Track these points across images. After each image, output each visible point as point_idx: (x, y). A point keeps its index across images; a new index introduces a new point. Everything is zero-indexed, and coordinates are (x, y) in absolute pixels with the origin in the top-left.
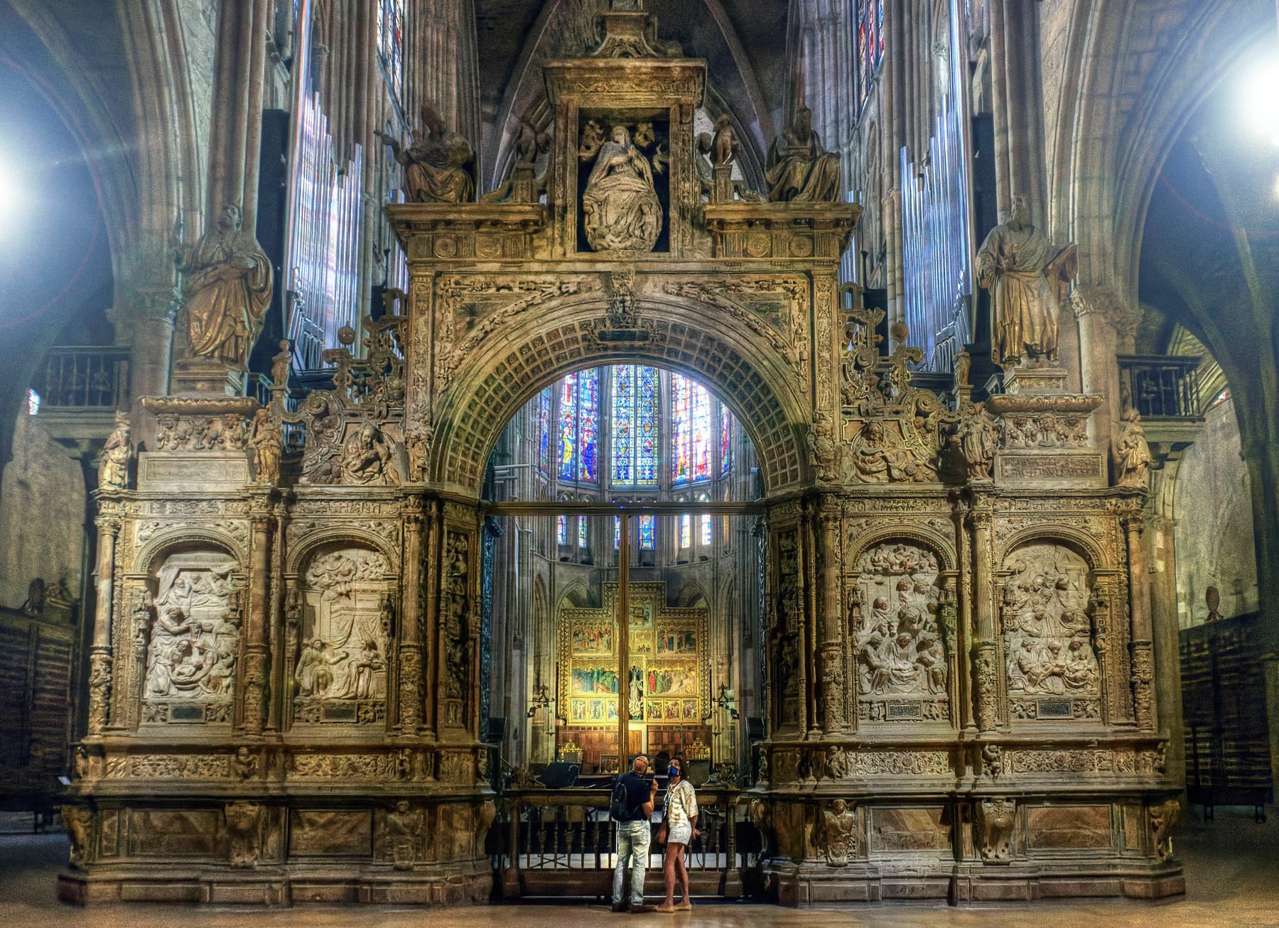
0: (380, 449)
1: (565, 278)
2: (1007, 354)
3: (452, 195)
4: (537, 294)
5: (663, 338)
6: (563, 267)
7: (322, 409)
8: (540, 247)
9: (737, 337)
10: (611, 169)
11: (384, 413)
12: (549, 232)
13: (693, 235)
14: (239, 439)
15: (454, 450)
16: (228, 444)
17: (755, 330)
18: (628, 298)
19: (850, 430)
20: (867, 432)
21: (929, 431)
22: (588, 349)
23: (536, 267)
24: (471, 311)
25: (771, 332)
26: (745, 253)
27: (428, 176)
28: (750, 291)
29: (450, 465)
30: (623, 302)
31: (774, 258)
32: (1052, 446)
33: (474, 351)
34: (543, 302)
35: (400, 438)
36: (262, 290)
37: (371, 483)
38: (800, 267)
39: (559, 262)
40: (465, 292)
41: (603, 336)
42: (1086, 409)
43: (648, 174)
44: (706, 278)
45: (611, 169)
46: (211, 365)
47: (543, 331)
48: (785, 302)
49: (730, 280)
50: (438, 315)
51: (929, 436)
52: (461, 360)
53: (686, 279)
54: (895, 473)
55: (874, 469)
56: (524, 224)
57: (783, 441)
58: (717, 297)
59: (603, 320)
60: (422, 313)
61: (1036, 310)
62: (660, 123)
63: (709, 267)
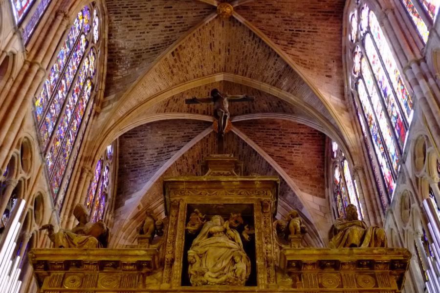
10: (210, 235)
13: (276, 276)
56: (139, 265)
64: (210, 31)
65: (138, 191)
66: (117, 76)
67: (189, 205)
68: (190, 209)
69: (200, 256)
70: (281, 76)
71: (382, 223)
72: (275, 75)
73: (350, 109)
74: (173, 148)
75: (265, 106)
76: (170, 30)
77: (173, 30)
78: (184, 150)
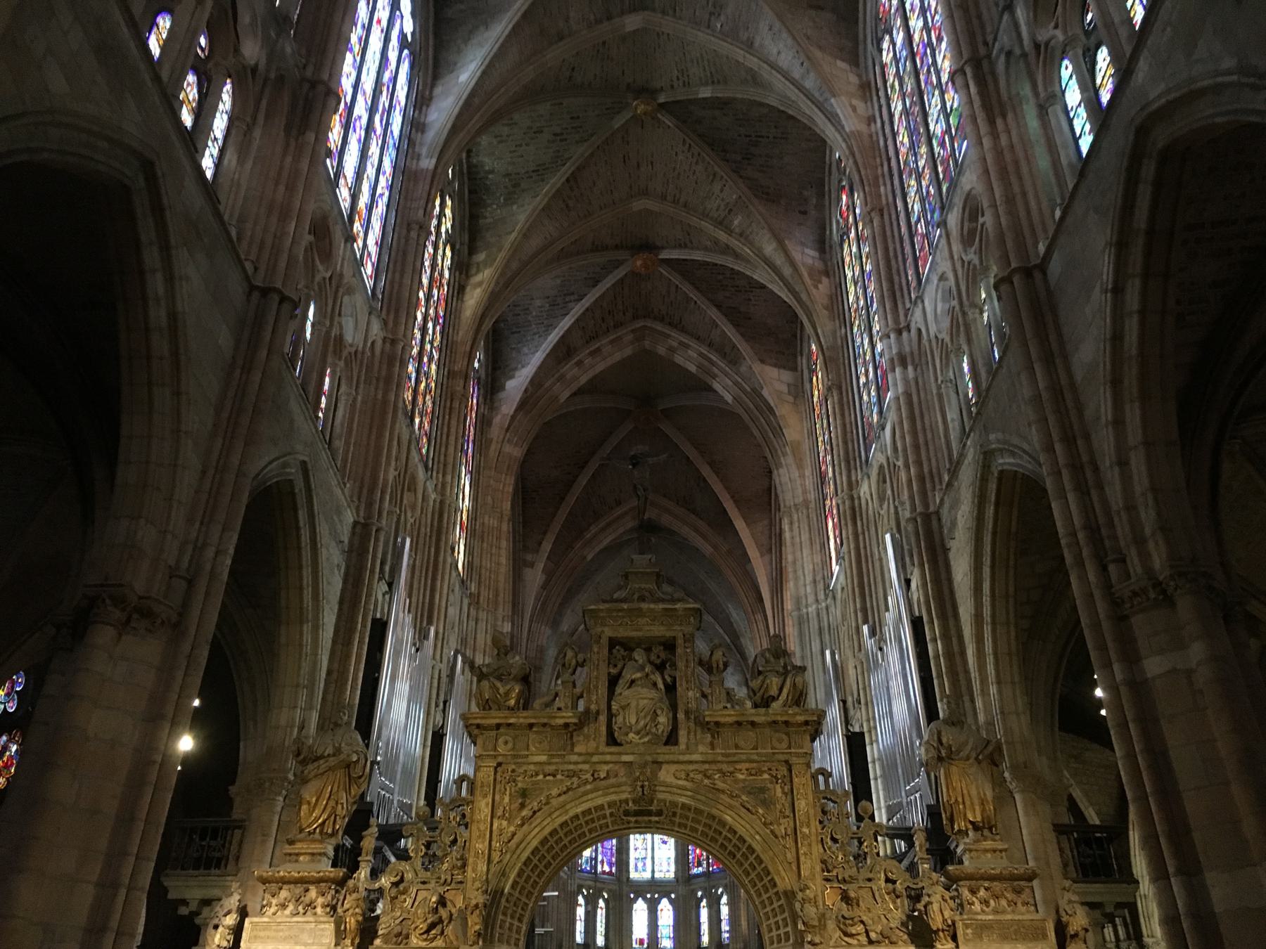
0: (443, 913)
1: (598, 767)
2: (956, 827)
3: (512, 702)
4: (575, 779)
5: (674, 814)
6: (595, 759)
7: (398, 877)
8: (578, 741)
9: (735, 816)
11: (449, 880)
12: (586, 730)
13: (695, 732)
14: (328, 906)
15: (505, 914)
16: (319, 910)
17: (748, 810)
18: (646, 783)
19: (830, 897)
20: (846, 898)
21: (898, 897)
22: (614, 823)
23: (574, 758)
24: (524, 794)
25: (761, 811)
26: (737, 747)
27: (494, 687)
28: (741, 777)
29: (500, 927)
30: (642, 787)
31: (759, 751)
32: (1004, 912)
33: (525, 827)
34: (579, 786)
35: (460, 903)
36: (360, 777)
37: (434, 944)
38: (782, 757)
39: (592, 755)
40: (520, 779)
41: (627, 813)
42: (1030, 878)
43: (661, 686)
44: (707, 766)
45: (633, 682)
46: (314, 841)
47: (579, 810)
48: (769, 785)
49: (725, 767)
50: (497, 797)
51: (898, 901)
52: (514, 834)
53: (691, 767)
54: (873, 935)
55: (854, 932)
56: (566, 725)
57: (776, 905)
58: (716, 782)
59: (626, 801)
60: (485, 796)
61: (974, 792)
62: (670, 646)
63: (710, 758)
64: (623, 138)
65: (523, 367)
66: (486, 218)
67: (610, 638)
68: (613, 643)
69: (623, 708)
70: (731, 210)
71: (857, 481)
72: (722, 207)
73: (831, 273)
74: (572, 298)
75: (709, 243)
76: (561, 140)
77: (566, 140)
78: (586, 302)
